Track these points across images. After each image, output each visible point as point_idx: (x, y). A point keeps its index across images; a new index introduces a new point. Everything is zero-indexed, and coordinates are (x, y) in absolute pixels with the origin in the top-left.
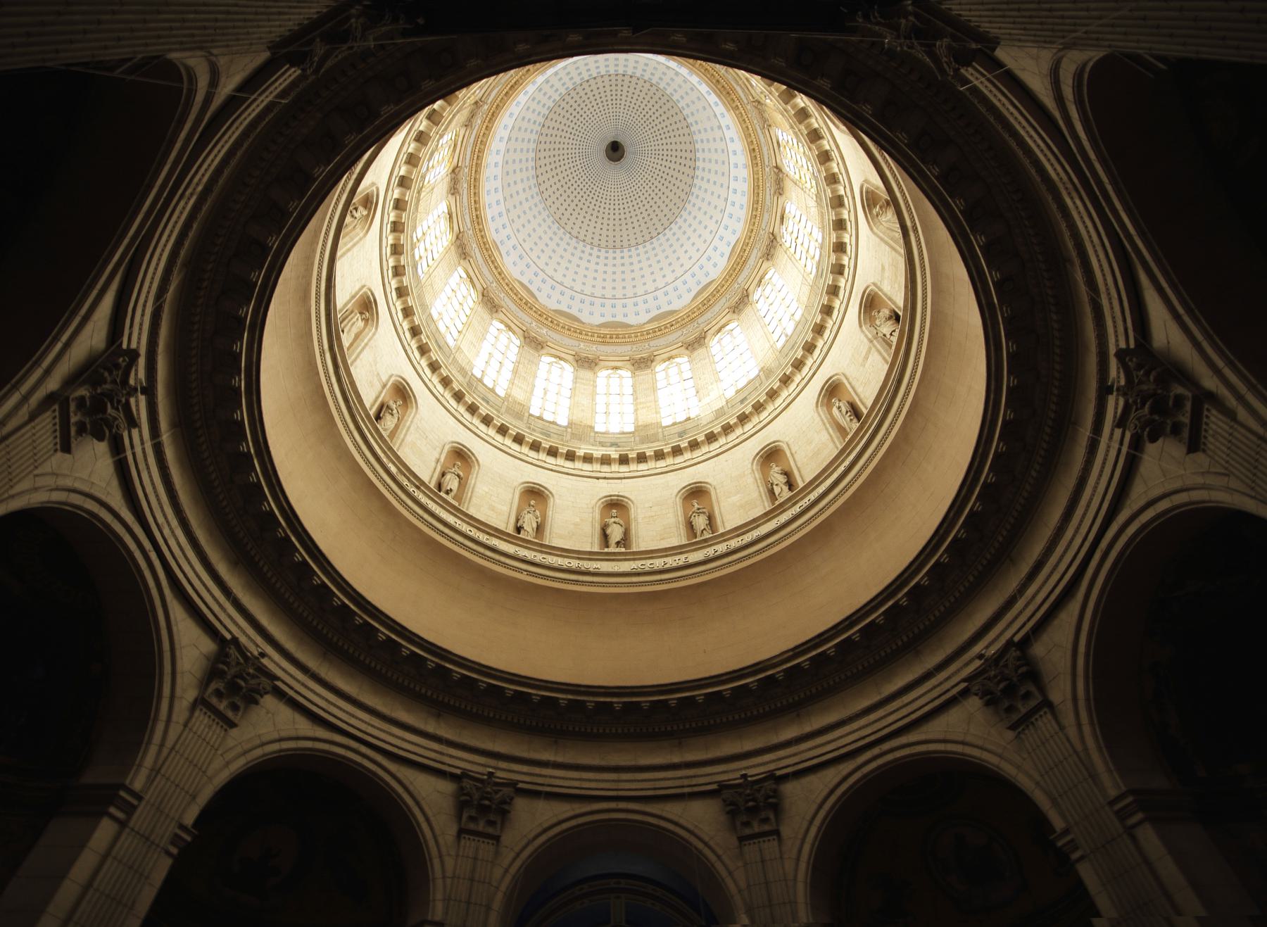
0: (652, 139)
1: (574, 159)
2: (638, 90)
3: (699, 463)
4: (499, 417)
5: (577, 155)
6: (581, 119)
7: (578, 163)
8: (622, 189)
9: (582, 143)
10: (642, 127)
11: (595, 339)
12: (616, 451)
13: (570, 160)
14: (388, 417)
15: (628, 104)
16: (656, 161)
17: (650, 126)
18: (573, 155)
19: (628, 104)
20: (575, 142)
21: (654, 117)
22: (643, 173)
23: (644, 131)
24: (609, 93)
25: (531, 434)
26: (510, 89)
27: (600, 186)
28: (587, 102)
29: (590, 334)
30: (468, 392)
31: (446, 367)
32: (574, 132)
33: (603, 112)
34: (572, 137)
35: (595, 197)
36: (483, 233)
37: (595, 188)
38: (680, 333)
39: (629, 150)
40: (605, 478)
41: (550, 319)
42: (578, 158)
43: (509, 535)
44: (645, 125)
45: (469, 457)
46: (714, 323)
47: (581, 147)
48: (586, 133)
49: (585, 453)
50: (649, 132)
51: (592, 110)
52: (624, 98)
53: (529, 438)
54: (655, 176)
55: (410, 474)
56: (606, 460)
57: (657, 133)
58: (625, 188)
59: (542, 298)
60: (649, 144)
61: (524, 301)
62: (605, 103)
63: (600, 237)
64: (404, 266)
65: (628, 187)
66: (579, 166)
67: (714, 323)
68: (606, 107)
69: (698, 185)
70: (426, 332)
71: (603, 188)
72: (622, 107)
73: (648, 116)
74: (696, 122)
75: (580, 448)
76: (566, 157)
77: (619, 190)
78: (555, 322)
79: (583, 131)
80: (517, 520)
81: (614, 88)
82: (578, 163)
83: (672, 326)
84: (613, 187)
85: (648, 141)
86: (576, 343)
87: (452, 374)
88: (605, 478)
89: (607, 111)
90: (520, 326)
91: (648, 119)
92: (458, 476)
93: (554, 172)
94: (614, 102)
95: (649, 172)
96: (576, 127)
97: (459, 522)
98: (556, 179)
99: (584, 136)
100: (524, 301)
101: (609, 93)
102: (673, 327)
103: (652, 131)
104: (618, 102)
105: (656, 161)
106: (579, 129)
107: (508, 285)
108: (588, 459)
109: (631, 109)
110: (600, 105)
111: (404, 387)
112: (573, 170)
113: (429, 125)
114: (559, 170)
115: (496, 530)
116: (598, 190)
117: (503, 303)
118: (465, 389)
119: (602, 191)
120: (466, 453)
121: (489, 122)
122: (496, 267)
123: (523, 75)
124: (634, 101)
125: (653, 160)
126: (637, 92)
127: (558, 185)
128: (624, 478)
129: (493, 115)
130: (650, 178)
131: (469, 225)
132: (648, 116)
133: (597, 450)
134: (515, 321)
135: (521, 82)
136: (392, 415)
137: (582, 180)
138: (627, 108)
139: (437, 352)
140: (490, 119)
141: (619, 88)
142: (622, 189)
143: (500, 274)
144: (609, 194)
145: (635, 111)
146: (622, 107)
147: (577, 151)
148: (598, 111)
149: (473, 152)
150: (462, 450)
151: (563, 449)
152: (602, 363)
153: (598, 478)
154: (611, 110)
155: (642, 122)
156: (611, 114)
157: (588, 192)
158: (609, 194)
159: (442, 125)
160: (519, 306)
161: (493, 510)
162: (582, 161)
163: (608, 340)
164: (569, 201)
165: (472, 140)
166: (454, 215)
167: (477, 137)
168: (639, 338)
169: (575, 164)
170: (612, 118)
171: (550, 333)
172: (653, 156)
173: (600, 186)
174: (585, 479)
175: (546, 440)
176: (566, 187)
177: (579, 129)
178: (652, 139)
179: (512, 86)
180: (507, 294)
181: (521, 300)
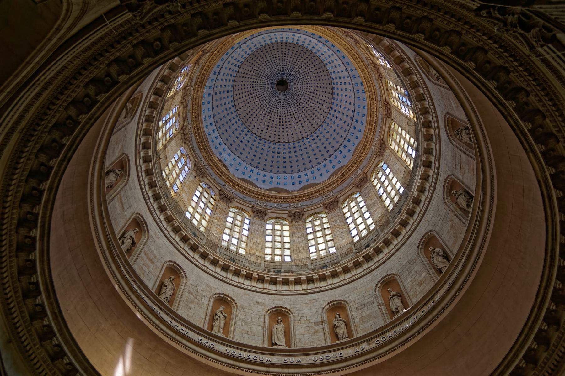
0: (276, 63)
1: (284, 112)
2: (248, 72)
3: (436, 112)
4: (378, 242)
5: (281, 110)
6: (262, 106)
7: (286, 110)
8: (304, 83)
9: (275, 107)
10: (269, 69)
11: (371, 137)
12: (420, 168)
13: (284, 115)
14: (338, 330)
15: (255, 78)
16: (288, 61)
17: (269, 64)
18: (281, 113)
19: (255, 78)
20: (274, 111)
21: (263, 62)
22: (295, 69)
23: (271, 68)
24: (249, 89)
25: (395, 224)
26: (219, 171)
27: (300, 97)
28: (253, 102)
29: (367, 140)
30: (357, 258)
31: (338, 267)
32: (268, 111)
33: (260, 93)
34: (271, 113)
35: (306, 101)
36: (294, 197)
37: (301, 101)
38: (373, 77)
39: (282, 77)
40: (435, 184)
41: (353, 165)
42: (283, 110)
43: (440, 281)
44: (268, 67)
45: (391, 278)
46: (367, 56)
47: (277, 107)
48: (270, 104)
49: (417, 190)
50: (272, 65)
51: (257, 100)
52: (252, 80)
53: (397, 227)
54: (297, 62)
55: (373, 334)
56: (425, 178)
57: (272, 59)
58: (303, 81)
59: (344, 162)
60: (279, 65)
61: (338, 179)
62: (255, 91)
63: (297, 135)
64: (271, 278)
65: (302, 79)
66: (288, 109)
67: (367, 56)
68: (257, 91)
69: (297, 41)
70: (313, 274)
71: (301, 96)
72: (257, 81)
73: (263, 65)
74: (260, 43)
75: (413, 193)
76: (281, 118)
77: (304, 85)
78: (355, 161)
79: (268, 106)
80: (434, 268)
81: (246, 87)
82: (286, 110)
83: (369, 82)
84: (301, 89)
85: (277, 65)
86: (371, 151)
87: (343, 264)
88: (435, 184)
89: (259, 90)
90: (351, 187)
91: (265, 65)
92: (394, 296)
93: (289, 126)
94: (254, 86)
95: (294, 66)
96: (266, 110)
97: (415, 317)
98: (292, 126)
99: (271, 105)
100: (338, 179)
101: (249, 89)
102: (370, 81)
103: (271, 63)
104: (254, 83)
105: (288, 61)
106: (267, 108)
107: (327, 187)
108: (421, 190)
109: (259, 76)
110: (255, 94)
111: (333, 304)
112: (289, 114)
113: (197, 252)
114: (288, 123)
115: (430, 292)
116: (302, 99)
117: (335, 195)
118: (354, 259)
119: (303, 97)
120: (387, 279)
121: (235, 184)
122: (316, 193)
123: (213, 163)
124: (254, 74)
125: (288, 63)
126: (249, 72)
127: (296, 125)
128: (438, 169)
129: (232, 182)
130: (298, 65)
131: (288, 205)
132: (263, 65)
133: (417, 181)
134: (347, 190)
135: (216, 164)
136: (338, 327)
137: (295, 109)
138: (258, 78)
139: (327, 270)
140: (233, 183)
141: (246, 83)
142: (304, 83)
143: (320, 191)
144: (304, 94)
145: (260, 73)
146: (257, 81)
147: (279, 110)
148: (258, 96)
149: (249, 196)
150: (384, 281)
151: (410, 205)
152: (385, 138)
153: (435, 189)
154: (259, 88)
155: (266, 69)
156: (261, 88)
157: (303, 106)
158: (305, 92)
159: (199, 244)
160: (341, 183)
161: (422, 284)
162: (285, 107)
163: (373, 128)
164: (306, 120)
165: (242, 196)
166: (278, 215)
167: (242, 192)
168: (375, 106)
169: (286, 112)
170: (263, 87)
171: (361, 167)
172: (286, 62)
173: (300, 97)
174: (433, 198)
175: (402, 215)
176: (298, 120)
177: (267, 108)
178: (276, 63)
179: (218, 169)
180: (332, 189)
181: (338, 181)
